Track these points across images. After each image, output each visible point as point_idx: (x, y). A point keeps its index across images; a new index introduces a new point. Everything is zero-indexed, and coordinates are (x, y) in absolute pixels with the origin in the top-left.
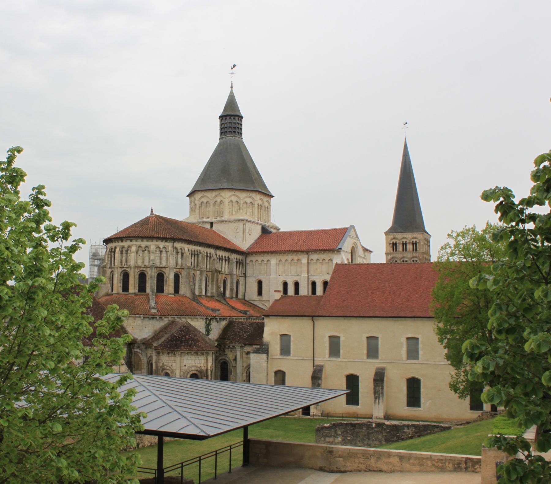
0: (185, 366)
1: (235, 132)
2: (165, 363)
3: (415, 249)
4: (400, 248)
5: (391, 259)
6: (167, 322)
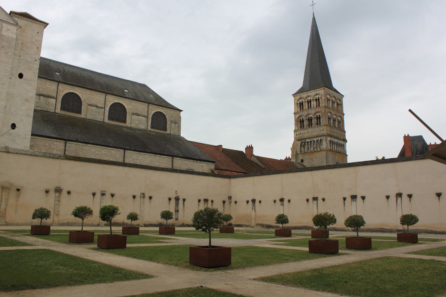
3: (318, 105)
4: (306, 106)
5: (299, 117)
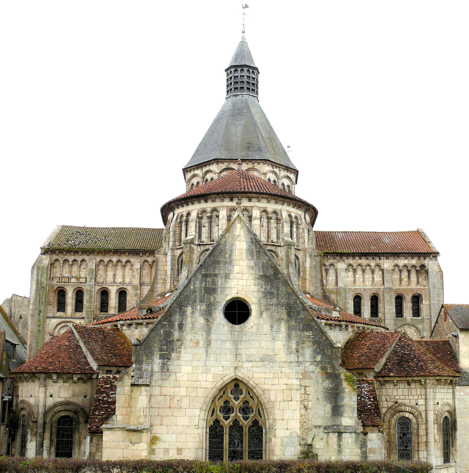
0: (438, 404)
1: (253, 90)
2: (400, 401)
6: (351, 334)
